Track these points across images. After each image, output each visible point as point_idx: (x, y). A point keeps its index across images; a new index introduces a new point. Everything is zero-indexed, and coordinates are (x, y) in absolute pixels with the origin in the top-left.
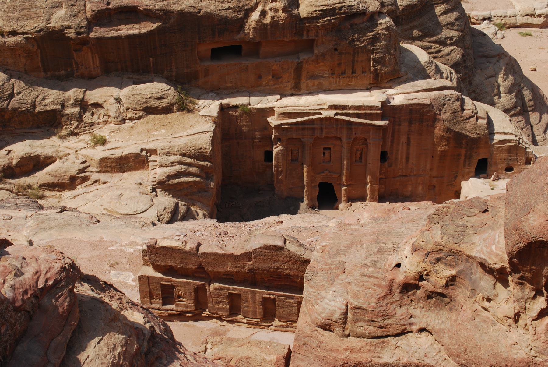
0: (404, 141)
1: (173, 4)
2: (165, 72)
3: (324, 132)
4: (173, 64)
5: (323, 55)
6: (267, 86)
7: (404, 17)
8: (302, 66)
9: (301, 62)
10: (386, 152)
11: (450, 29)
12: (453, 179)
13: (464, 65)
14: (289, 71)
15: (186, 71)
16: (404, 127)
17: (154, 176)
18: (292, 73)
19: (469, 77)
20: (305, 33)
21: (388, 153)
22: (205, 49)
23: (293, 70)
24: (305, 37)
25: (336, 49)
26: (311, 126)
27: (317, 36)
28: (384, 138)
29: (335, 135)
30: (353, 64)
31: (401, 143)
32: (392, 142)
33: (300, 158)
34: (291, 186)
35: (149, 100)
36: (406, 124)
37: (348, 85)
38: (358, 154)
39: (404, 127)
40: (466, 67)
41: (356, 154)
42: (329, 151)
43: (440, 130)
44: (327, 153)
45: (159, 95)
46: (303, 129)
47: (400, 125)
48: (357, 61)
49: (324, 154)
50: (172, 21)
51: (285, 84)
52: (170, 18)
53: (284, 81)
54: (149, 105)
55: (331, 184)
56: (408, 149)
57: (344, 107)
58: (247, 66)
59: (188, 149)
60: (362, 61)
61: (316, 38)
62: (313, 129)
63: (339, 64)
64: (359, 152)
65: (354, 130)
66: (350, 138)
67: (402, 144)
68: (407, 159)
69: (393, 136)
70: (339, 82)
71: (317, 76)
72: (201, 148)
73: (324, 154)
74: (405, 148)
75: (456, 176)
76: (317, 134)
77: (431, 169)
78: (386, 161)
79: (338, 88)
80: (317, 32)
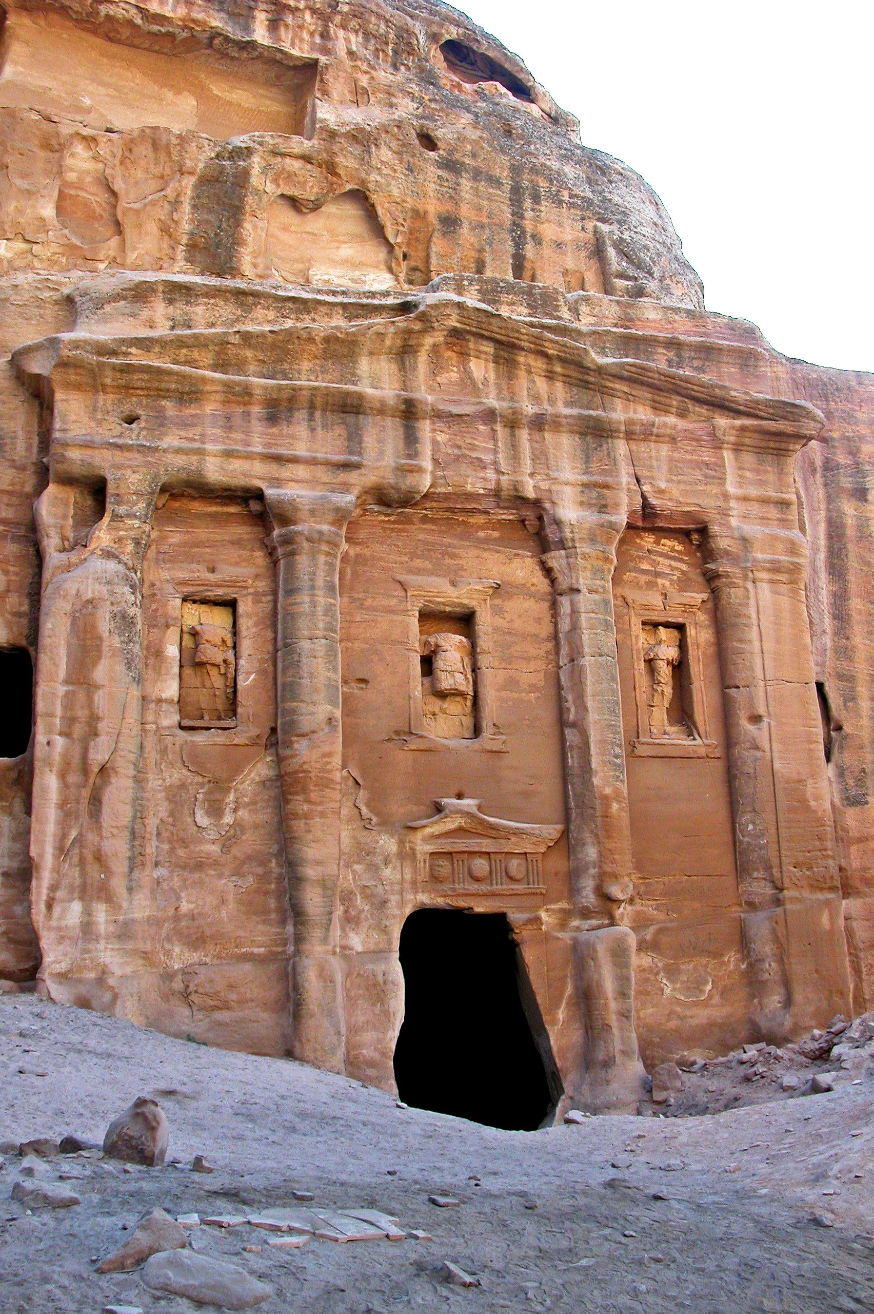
3: (426, 450)
14: (170, 192)
18: (187, 208)
23: (189, 182)
25: (428, 141)
30: (519, 243)
34: (180, 957)
38: (665, 672)
41: (650, 663)
48: (538, 240)
49: (428, 664)
53: (131, 257)
55: (498, 924)
60: (559, 245)
61: (323, 59)
64: (669, 652)
65: (621, 447)
66: (603, 508)
73: (428, 664)
80: (325, 35)
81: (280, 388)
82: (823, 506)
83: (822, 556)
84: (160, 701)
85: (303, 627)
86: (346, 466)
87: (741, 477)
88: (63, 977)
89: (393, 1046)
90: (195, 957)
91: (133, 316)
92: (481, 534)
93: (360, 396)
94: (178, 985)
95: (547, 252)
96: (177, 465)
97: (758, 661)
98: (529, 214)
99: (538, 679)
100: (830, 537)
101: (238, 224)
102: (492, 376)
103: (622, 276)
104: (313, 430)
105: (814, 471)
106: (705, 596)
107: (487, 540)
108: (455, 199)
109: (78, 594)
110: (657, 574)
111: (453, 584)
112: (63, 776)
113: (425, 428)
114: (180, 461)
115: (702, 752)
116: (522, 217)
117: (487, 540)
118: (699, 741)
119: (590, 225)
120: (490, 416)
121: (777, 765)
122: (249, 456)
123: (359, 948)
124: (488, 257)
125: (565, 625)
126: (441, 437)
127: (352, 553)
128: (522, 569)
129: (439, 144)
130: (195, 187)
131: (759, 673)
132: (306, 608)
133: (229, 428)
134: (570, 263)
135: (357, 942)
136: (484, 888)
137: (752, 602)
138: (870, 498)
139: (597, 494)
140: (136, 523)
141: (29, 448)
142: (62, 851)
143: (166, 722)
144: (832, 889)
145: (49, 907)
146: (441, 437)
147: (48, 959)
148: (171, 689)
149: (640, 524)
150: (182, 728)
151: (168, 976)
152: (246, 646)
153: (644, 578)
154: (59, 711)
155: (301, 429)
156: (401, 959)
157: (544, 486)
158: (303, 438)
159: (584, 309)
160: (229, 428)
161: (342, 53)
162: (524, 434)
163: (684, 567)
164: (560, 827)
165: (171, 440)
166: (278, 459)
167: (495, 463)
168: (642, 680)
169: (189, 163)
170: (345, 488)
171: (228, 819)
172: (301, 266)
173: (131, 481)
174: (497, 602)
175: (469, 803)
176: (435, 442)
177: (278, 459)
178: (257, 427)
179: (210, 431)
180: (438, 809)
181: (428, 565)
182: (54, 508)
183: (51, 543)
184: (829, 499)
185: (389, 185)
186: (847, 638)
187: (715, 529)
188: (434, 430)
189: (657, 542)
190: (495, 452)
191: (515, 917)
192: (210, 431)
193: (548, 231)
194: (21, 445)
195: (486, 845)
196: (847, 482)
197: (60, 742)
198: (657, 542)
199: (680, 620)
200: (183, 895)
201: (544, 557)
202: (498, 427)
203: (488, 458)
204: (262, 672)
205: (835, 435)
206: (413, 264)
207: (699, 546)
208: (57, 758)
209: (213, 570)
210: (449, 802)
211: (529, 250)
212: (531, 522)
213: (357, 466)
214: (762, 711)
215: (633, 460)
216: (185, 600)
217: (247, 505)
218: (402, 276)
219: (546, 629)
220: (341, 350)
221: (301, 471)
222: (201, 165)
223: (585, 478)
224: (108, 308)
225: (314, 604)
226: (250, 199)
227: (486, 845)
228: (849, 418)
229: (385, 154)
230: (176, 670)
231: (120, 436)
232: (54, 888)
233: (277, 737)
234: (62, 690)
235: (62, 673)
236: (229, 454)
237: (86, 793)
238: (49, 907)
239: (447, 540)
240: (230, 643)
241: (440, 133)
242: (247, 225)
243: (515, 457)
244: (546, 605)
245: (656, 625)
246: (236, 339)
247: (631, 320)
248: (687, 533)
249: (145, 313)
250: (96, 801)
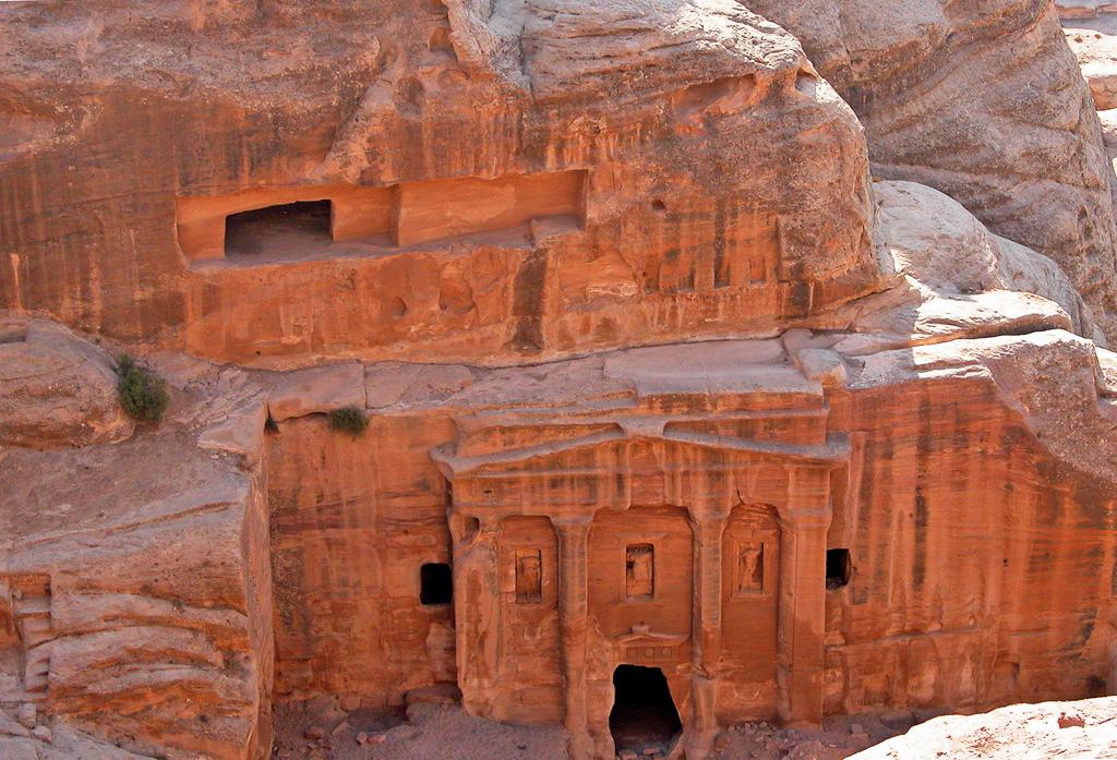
0: (907, 513)
1: (89, 62)
2: (67, 302)
3: (628, 492)
4: (95, 273)
5: (616, 224)
6: (426, 336)
7: (875, 88)
8: (545, 264)
9: (543, 252)
10: (845, 551)
11: (1033, 124)
12: (1080, 638)
13: (1086, 245)
14: (501, 283)
15: (138, 295)
16: (904, 461)
17: (42, 668)
18: (511, 290)
19: (1105, 285)
20: (551, 152)
21: (853, 556)
22: (206, 213)
23: (511, 279)
24: (551, 163)
25: (659, 204)
26: (583, 472)
27: (593, 160)
28: (837, 504)
29: (668, 502)
30: (719, 251)
31: (895, 521)
32: (864, 518)
33: (545, 583)
34: (518, 686)
35: (11, 402)
36: (913, 451)
37: (701, 324)
39: (904, 461)
40: (1091, 251)
42: (648, 555)
43: (1025, 468)
44: (641, 562)
45: (50, 384)
46: (555, 483)
47: (889, 456)
48: (733, 243)
49: (630, 565)
50: (86, 123)
51: (489, 329)
52: (80, 115)
54: (16, 417)
56: (920, 539)
57: (695, 402)
58: (354, 273)
59: (160, 568)
60: (748, 241)
61: (591, 168)
62: (590, 481)
63: (672, 255)
65: (731, 479)
67: (900, 521)
68: (919, 571)
69: (865, 495)
70: (674, 314)
71: (598, 297)
72: (206, 564)
73: (630, 565)
74: (909, 534)
75: (1090, 627)
76: (606, 497)
77: (1004, 605)
78: (845, 583)
79: (670, 338)
80: (593, 146)
82: (861, 467)
83: (857, 490)
84: (507, 593)
85: (569, 574)
86: (589, 504)
87: (798, 485)
88: (471, 702)
90: (525, 686)
91: (486, 441)
92: (659, 511)
94: (518, 696)
95: (739, 249)
96: (512, 510)
97: (794, 571)
98: (728, 227)
99: (684, 573)
100: (863, 481)
101: (542, 287)
102: (664, 452)
103: (791, 258)
104: (572, 488)
105: (858, 448)
107: (661, 514)
108: (676, 239)
109: (470, 569)
110: (750, 521)
112: (468, 635)
113: (628, 483)
114: (512, 509)
116: (724, 231)
117: (661, 514)
118: (764, 595)
119: (772, 219)
120: (661, 473)
121: (797, 616)
122: (543, 504)
124: (697, 267)
125: (696, 555)
126: (635, 485)
128: (679, 525)
129: (667, 206)
130: (517, 279)
131: (794, 576)
132: (570, 565)
133: (533, 492)
134: (755, 251)
135: (594, 677)
136: (651, 660)
137: (795, 543)
138: (894, 457)
139: (716, 506)
141: (442, 487)
142: (469, 661)
144: (821, 665)
145: (465, 680)
146: (635, 485)
147: (465, 696)
148: (513, 588)
151: (514, 693)
152: (545, 568)
153: (743, 523)
154: (465, 614)
155: (567, 490)
158: (568, 494)
159: (720, 402)
160: (533, 492)
161: (604, 157)
162: (679, 479)
163: (766, 516)
164: (686, 637)
165: (507, 500)
166: (557, 505)
167: (663, 493)
169: (510, 267)
170: (588, 514)
171: (538, 637)
172: (580, 286)
173: (489, 519)
174: (665, 541)
175: (645, 628)
176: (633, 488)
177: (557, 505)
178: (546, 490)
179: (524, 494)
180: (631, 632)
181: (631, 527)
182: (455, 526)
183: (456, 538)
184: (866, 462)
185: (632, 247)
186: (866, 528)
188: (633, 482)
190: (664, 487)
191: (665, 672)
192: (524, 494)
193: (741, 235)
194: (438, 486)
195: (652, 644)
196: (879, 451)
197: (466, 624)
202: (666, 477)
203: (659, 491)
204: (552, 580)
205: (877, 427)
206: (649, 277)
208: (465, 630)
210: (635, 628)
211: (727, 253)
213: (595, 504)
214: (792, 591)
215: (736, 483)
218: (643, 284)
219: (689, 551)
220: (587, 456)
221: (568, 508)
222: (518, 268)
223: (709, 497)
224: (473, 437)
225: (573, 563)
226: (548, 274)
227: (652, 644)
228: (890, 415)
229: (631, 227)
231: (483, 501)
232: (466, 674)
233: (558, 605)
234: (465, 606)
235: (465, 598)
236: (534, 504)
237: (477, 641)
238: (465, 680)
239: (641, 516)
240: (538, 563)
241: (669, 197)
242: (547, 287)
243: (674, 490)
244: (689, 542)
247: (746, 404)
249: (491, 440)
250: (482, 644)
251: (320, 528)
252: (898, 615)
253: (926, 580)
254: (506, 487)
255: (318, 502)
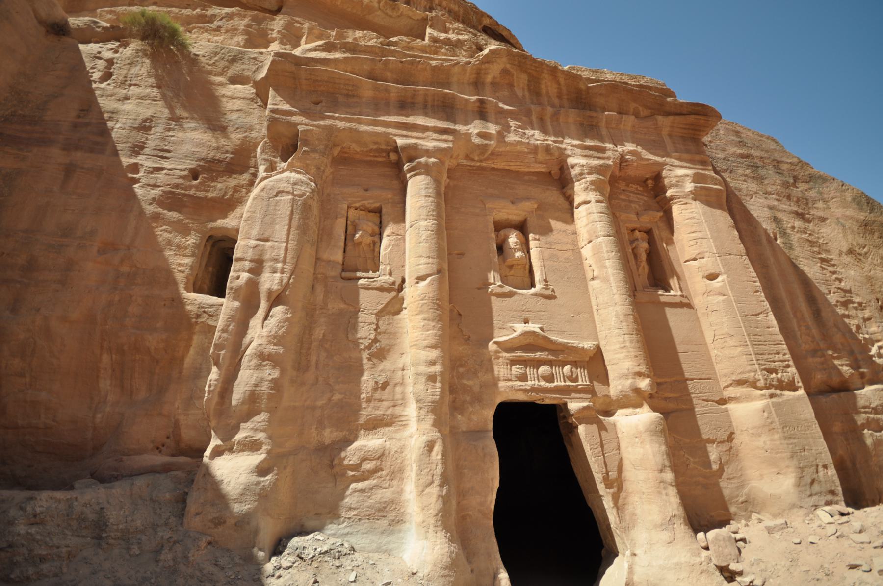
38: (644, 257)
81: (406, 90)
89: (493, 508)
92: (527, 178)
93: (454, 97)
102: (527, 93)
106: (661, 214)
111: (513, 203)
115: (678, 300)
123: (464, 429)
127: (451, 184)
140: (317, 156)
143: (332, 274)
148: (339, 257)
149: (617, 173)
150: (343, 278)
153: (623, 204)
156: (494, 436)
157: (563, 146)
163: (645, 199)
168: (631, 257)
187: (664, 173)
189: (627, 185)
198: (627, 185)
199: (649, 226)
200: (337, 387)
201: (564, 190)
207: (653, 189)
209: (366, 190)
212: (555, 171)
216: (349, 207)
217: (389, 156)
230: (342, 244)
245: (633, 230)
246: (380, 65)
248: (647, 179)
251: (64, 149)
252: (818, 360)
253: (823, 314)
254: (341, 99)
255: (79, 117)
